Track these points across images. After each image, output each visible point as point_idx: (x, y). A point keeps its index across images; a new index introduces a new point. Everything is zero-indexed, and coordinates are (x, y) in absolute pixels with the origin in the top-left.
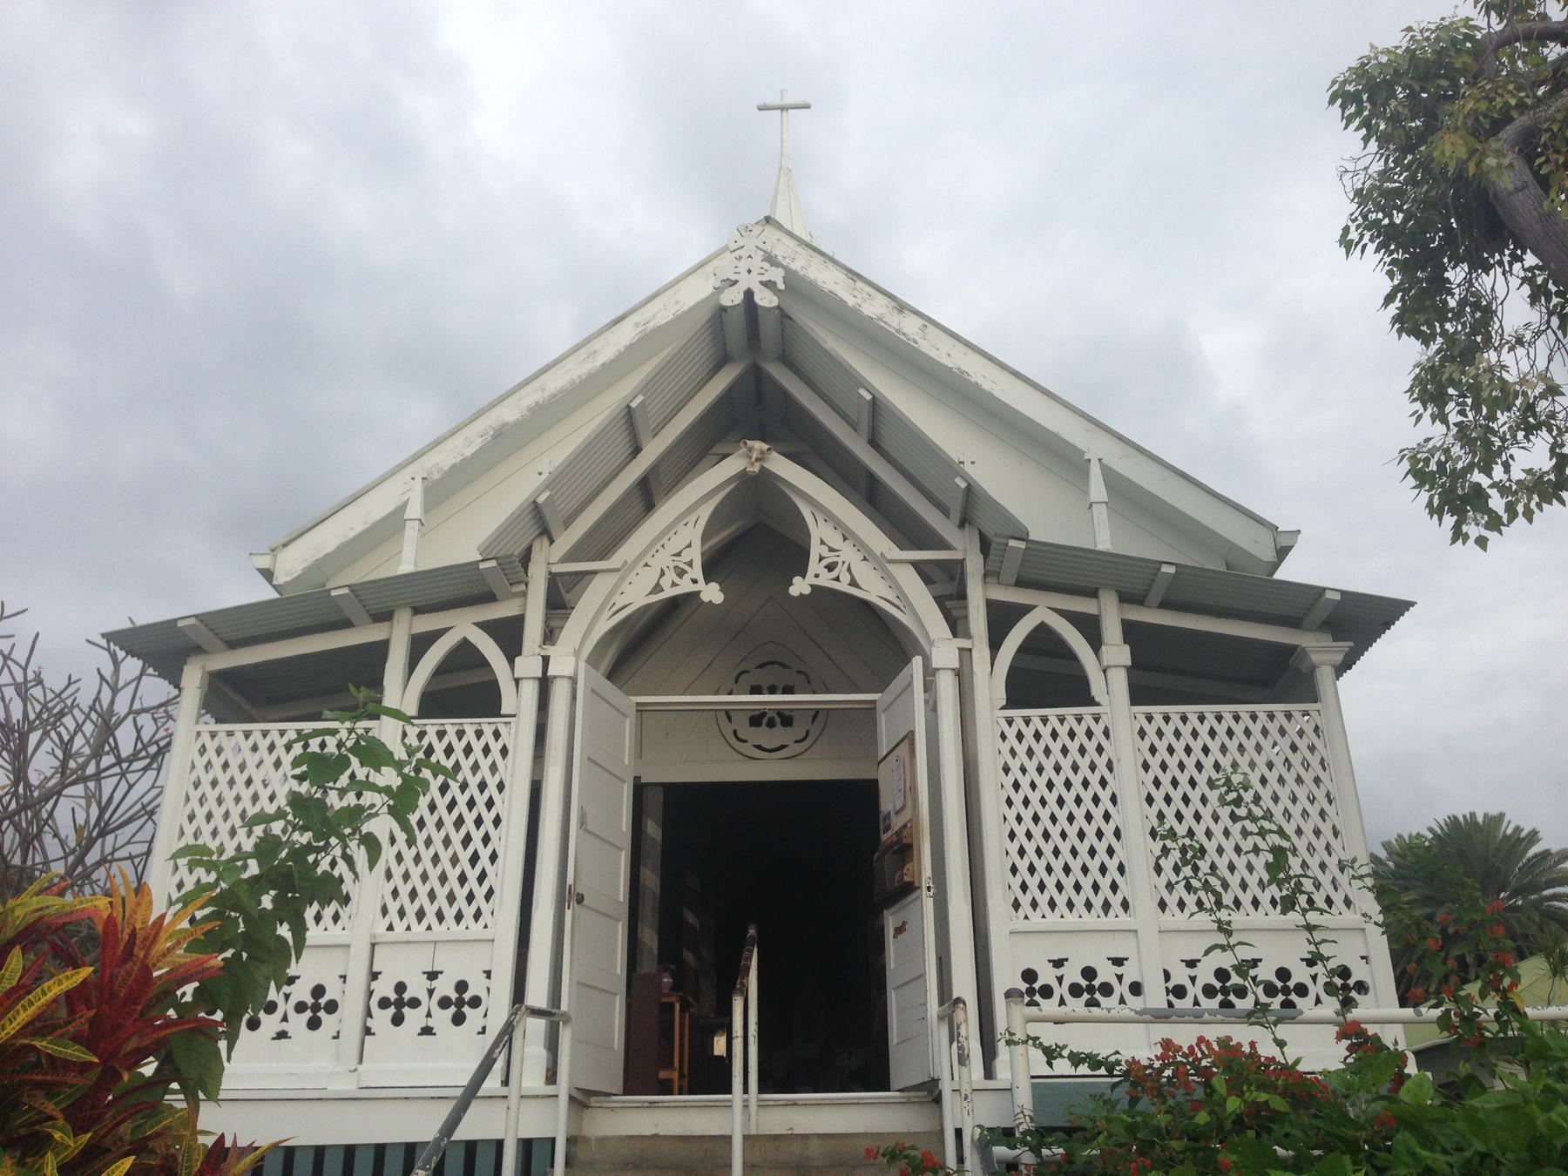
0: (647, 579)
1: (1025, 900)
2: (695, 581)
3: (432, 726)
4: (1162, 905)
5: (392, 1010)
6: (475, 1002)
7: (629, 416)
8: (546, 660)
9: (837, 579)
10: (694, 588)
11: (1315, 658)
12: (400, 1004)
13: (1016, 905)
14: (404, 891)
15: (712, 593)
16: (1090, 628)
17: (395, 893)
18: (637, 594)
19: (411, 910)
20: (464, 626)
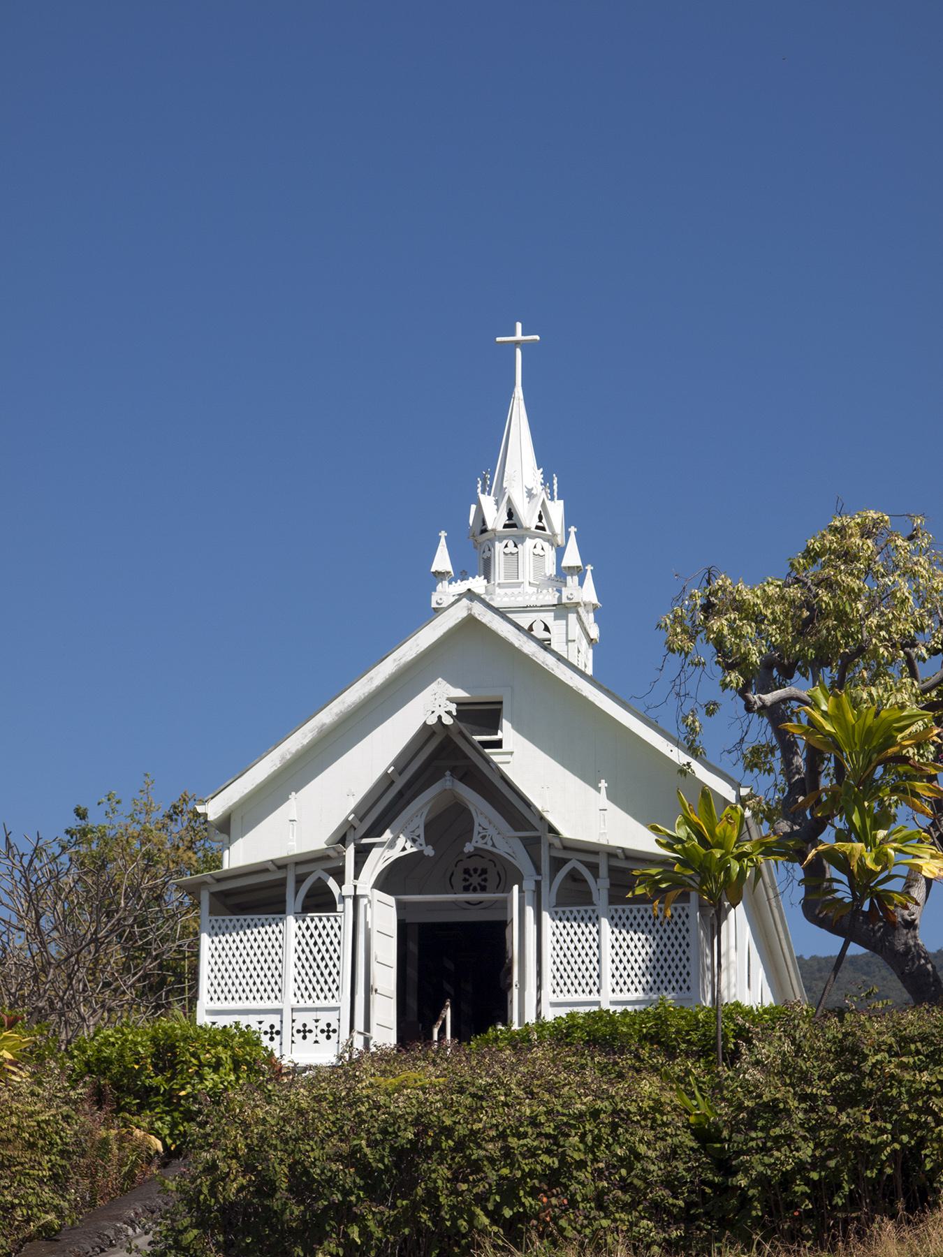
1: (558, 989)
2: (421, 845)
4: (613, 991)
5: (302, 1034)
8: (355, 887)
9: (486, 843)
12: (304, 1031)
16: (593, 868)
19: (306, 994)
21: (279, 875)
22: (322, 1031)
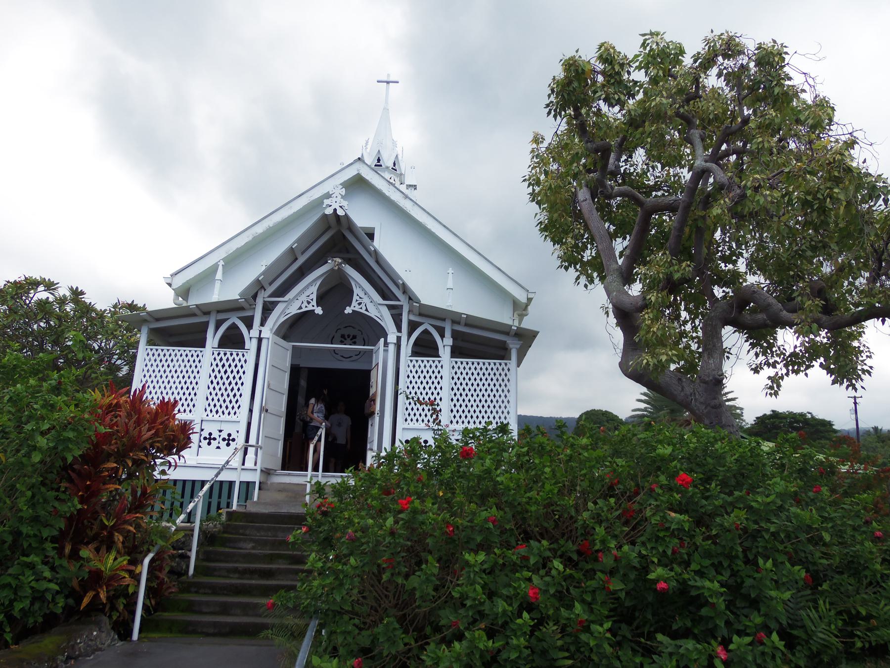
0: (297, 304)
3: (222, 351)
5: (208, 441)
6: (234, 440)
7: (291, 250)
8: (260, 331)
10: (313, 308)
11: (511, 346)
12: (210, 439)
13: (406, 420)
14: (212, 404)
15: (319, 311)
17: (209, 405)
18: (294, 310)
19: (214, 410)
20: (234, 319)
21: (204, 319)
22: (224, 439)
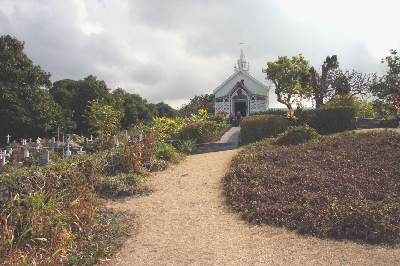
15: (238, 95)
16: (255, 97)
18: (234, 95)
